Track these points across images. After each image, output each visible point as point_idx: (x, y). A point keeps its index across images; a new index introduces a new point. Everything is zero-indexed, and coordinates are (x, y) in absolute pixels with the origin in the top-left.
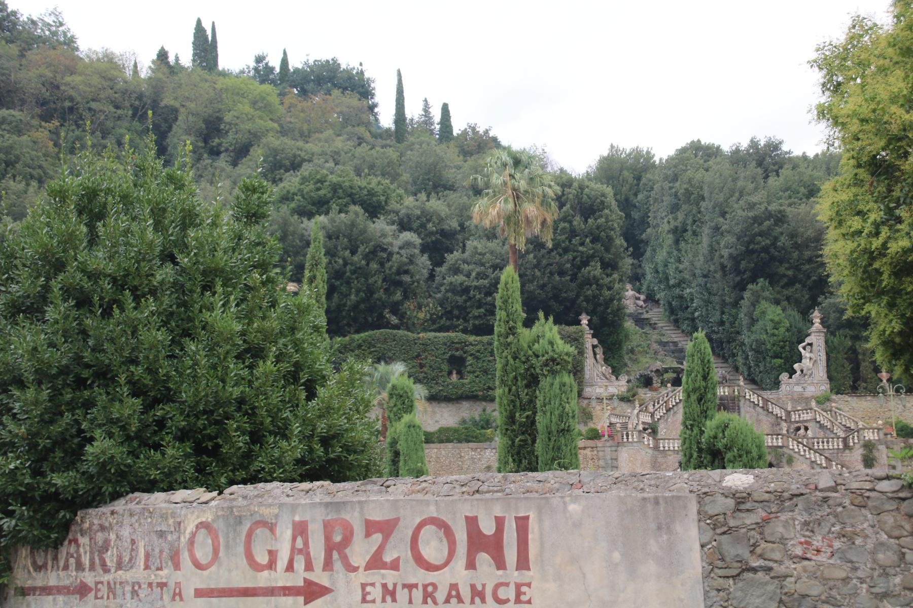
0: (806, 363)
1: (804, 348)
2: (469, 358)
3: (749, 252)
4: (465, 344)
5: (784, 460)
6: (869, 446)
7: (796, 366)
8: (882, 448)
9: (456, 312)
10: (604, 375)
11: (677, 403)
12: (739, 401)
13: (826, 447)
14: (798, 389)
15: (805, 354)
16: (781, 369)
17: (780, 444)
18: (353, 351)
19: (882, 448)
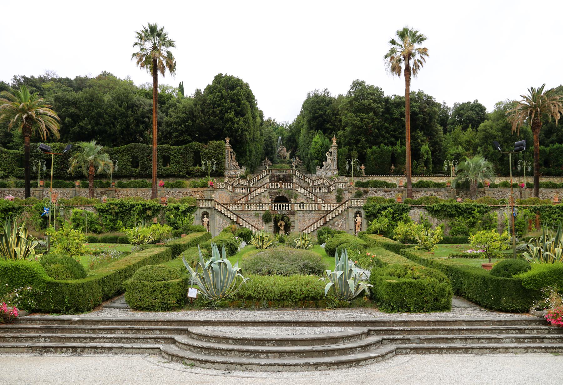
0: (328, 161)
1: (328, 155)
2: (171, 156)
3: (315, 118)
4: (171, 150)
5: (293, 196)
6: (340, 191)
7: (324, 163)
8: (346, 192)
9: (168, 136)
10: (235, 166)
11: (263, 177)
12: (293, 177)
13: (319, 192)
14: (324, 173)
15: (328, 157)
16: (317, 164)
17: (291, 188)
18: (121, 153)
19: (346, 192)
